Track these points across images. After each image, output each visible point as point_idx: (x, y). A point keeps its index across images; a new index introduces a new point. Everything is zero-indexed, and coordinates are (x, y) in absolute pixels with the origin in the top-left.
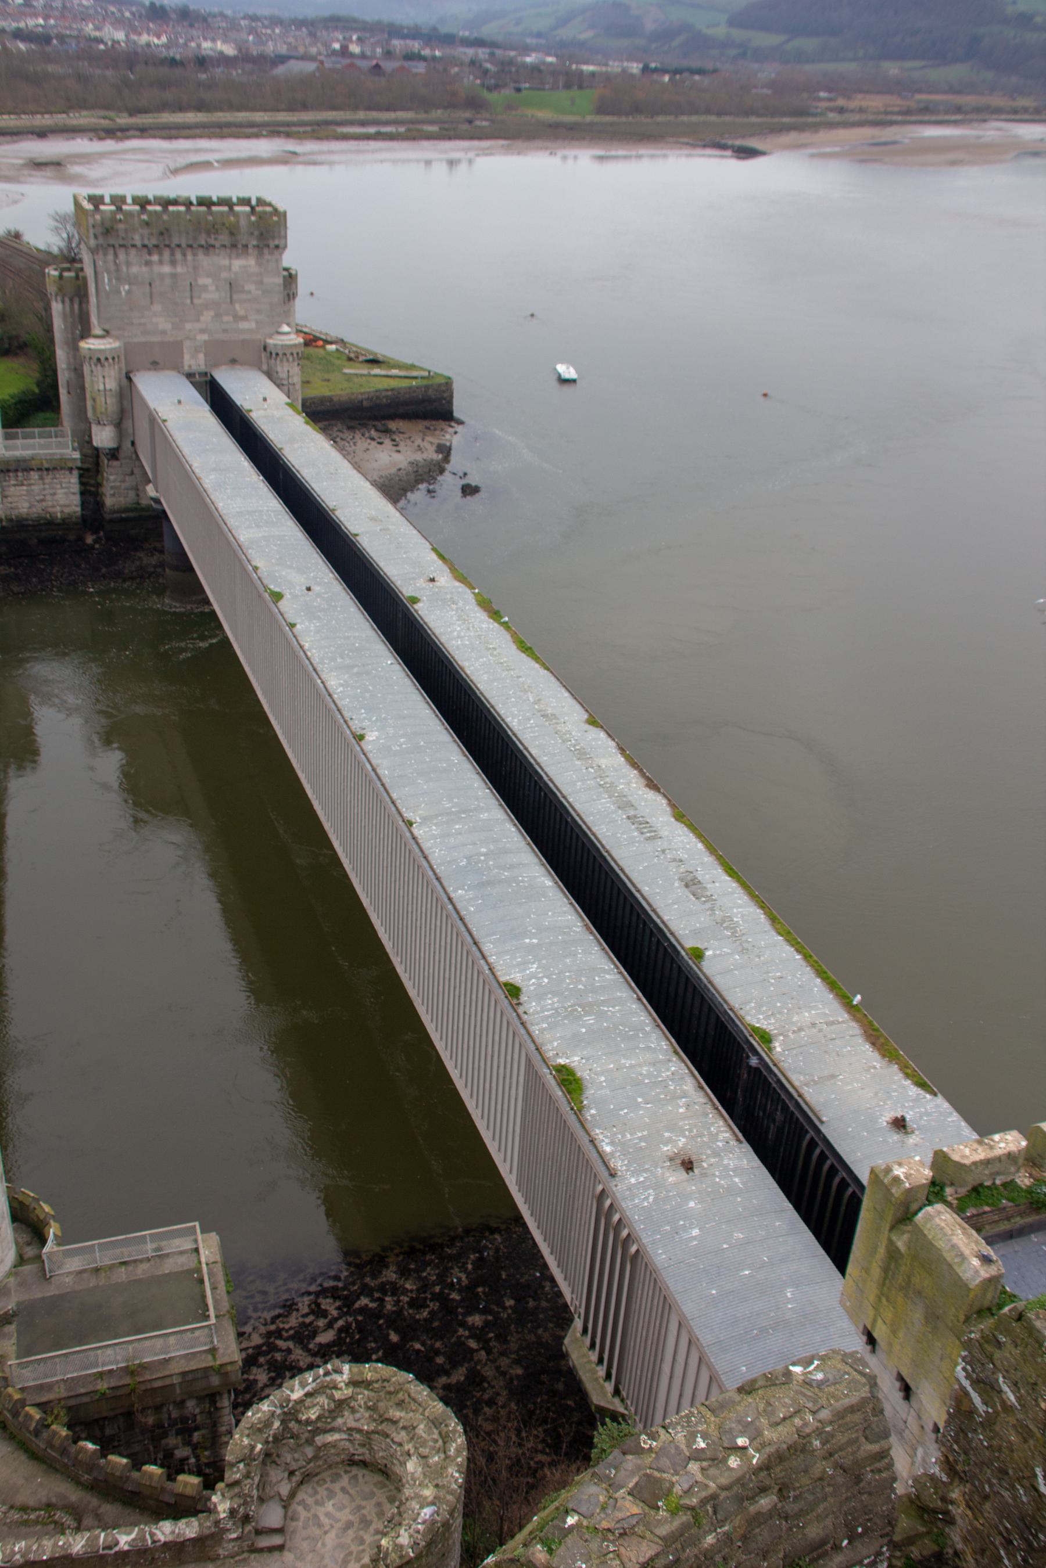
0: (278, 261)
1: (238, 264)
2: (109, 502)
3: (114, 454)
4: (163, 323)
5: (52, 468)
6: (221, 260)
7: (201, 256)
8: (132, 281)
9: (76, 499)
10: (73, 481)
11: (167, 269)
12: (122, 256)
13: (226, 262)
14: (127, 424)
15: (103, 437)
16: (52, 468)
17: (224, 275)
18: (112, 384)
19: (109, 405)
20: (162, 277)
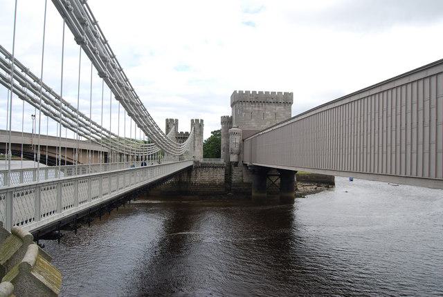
0: (290, 107)
1: (278, 108)
2: (234, 180)
3: (236, 164)
4: (254, 124)
5: (215, 167)
6: (273, 107)
7: (267, 106)
8: (246, 112)
9: (223, 178)
10: (223, 172)
11: (257, 109)
12: (244, 104)
13: (274, 107)
14: (241, 155)
15: (233, 158)
16: (215, 167)
17: (274, 111)
18: (238, 141)
19: (236, 148)
20: (255, 111)
